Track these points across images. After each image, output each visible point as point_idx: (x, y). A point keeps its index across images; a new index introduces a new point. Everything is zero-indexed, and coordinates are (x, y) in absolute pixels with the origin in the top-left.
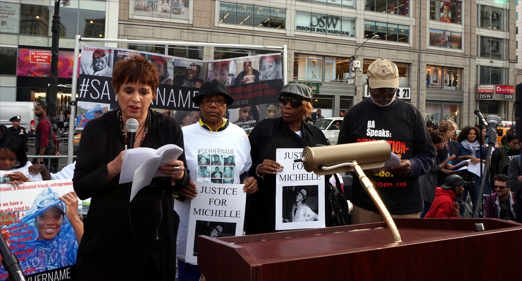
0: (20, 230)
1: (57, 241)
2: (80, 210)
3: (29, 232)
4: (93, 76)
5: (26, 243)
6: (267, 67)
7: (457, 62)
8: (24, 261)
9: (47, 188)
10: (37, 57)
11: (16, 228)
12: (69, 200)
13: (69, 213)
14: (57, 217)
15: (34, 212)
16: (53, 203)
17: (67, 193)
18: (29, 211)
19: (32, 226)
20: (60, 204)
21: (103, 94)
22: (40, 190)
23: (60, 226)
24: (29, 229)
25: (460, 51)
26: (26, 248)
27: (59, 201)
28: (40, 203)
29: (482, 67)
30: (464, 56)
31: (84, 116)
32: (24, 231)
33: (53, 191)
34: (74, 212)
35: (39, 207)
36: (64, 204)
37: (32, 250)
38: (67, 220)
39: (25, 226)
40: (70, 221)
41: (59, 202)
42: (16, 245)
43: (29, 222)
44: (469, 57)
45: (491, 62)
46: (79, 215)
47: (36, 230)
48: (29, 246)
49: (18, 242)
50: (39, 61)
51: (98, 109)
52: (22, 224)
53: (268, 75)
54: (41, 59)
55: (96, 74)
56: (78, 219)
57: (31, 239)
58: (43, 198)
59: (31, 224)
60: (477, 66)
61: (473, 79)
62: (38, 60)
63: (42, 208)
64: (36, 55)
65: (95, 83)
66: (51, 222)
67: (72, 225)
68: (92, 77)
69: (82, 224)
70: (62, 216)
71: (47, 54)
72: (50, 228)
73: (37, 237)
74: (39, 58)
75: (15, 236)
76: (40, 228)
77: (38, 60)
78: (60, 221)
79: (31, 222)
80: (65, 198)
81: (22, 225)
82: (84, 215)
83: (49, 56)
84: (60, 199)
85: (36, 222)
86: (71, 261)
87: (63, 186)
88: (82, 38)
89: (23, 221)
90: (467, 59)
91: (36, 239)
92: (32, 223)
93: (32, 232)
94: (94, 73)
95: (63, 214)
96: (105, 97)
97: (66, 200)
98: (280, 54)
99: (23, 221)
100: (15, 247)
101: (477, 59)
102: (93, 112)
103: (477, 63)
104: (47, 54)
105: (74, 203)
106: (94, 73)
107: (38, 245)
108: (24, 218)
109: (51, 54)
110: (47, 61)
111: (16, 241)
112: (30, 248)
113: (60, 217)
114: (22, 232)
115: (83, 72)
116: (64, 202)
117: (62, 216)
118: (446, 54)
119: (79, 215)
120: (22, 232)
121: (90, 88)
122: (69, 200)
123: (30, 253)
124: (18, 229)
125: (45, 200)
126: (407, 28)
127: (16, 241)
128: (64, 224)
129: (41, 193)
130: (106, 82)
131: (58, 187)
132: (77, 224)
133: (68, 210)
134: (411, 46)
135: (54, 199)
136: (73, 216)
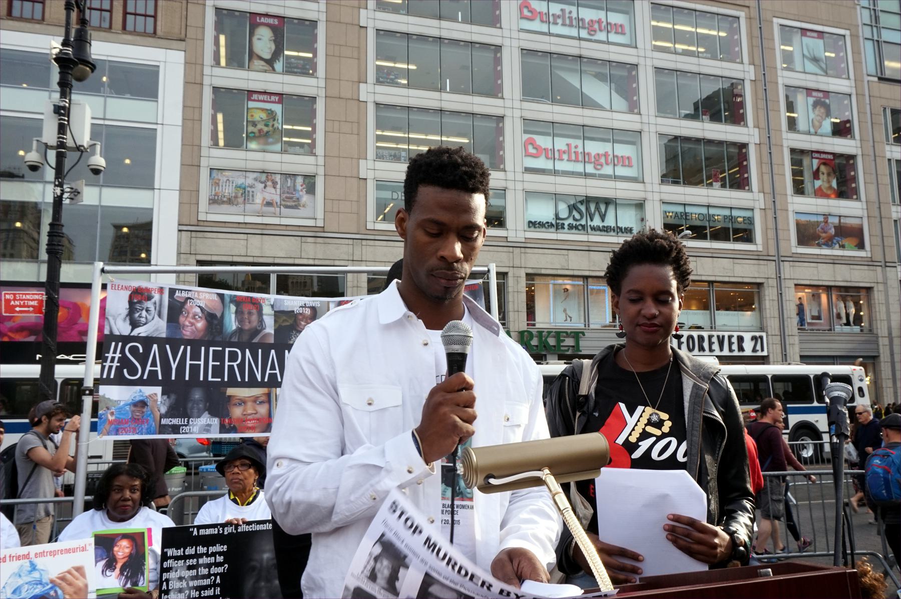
7: (858, 277)
9: (26, 560)
10: (17, 303)
12: (70, 584)
16: (38, 590)
17: (66, 570)
20: (52, 593)
25: (862, 254)
27: (50, 586)
28: (14, 592)
33: (39, 566)
36: (60, 592)
41: (51, 588)
44: (882, 264)
50: (21, 312)
54: (24, 306)
58: (20, 582)
62: (18, 309)
64: (15, 300)
74: (20, 306)
77: (18, 309)
80: (63, 579)
83: (42, 301)
84: (52, 581)
87: (59, 557)
90: (879, 269)
97: (64, 584)
98: (480, 281)
104: (36, 297)
105: (80, 589)
109: (44, 298)
110: (37, 310)
116: (61, 588)
118: (834, 261)
122: (70, 584)
125: (22, 585)
126: (748, 214)
129: (16, 571)
131: (49, 558)
134: (760, 248)
135: (40, 583)
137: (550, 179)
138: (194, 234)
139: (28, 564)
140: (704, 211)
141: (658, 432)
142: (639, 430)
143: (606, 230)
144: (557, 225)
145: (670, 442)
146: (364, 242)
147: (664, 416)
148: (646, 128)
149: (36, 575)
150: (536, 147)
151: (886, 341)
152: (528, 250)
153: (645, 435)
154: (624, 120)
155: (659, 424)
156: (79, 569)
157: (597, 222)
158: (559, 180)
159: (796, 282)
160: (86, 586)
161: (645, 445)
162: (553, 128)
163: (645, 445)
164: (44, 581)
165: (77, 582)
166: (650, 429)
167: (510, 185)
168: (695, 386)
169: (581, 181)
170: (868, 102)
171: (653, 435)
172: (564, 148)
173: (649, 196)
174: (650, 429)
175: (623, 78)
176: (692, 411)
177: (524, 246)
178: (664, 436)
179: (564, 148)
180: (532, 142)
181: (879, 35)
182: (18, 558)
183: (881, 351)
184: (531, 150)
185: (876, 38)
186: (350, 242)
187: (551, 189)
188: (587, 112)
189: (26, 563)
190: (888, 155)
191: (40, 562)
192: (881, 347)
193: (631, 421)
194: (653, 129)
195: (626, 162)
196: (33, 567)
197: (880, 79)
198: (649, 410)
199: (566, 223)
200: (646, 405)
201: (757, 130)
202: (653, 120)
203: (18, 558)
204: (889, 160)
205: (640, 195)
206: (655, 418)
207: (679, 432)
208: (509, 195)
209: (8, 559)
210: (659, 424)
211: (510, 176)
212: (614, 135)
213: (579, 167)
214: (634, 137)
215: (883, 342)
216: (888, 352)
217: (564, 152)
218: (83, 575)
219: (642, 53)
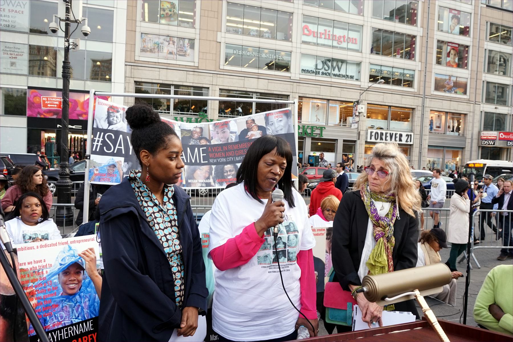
0: (45, 287)
3: (54, 288)
4: (107, 129)
5: (51, 299)
6: (275, 122)
7: (461, 108)
8: (51, 316)
9: (67, 245)
10: (49, 102)
11: (42, 285)
13: (88, 268)
14: (78, 273)
15: (56, 269)
16: (73, 260)
18: (52, 268)
19: (55, 282)
20: (80, 261)
21: (117, 147)
22: (62, 247)
23: (81, 281)
24: (53, 286)
25: (465, 97)
26: (52, 304)
27: (79, 257)
28: (62, 260)
29: (486, 113)
32: (49, 288)
34: (93, 268)
35: (61, 264)
36: (83, 260)
37: (57, 306)
38: (87, 275)
39: (49, 283)
42: (43, 301)
43: (53, 278)
45: (496, 108)
46: (98, 270)
47: (60, 286)
48: (55, 301)
49: (44, 298)
52: (46, 282)
53: (278, 129)
55: (111, 128)
57: (56, 295)
58: (65, 255)
59: (54, 281)
60: (481, 112)
62: (49, 105)
63: (64, 265)
64: (47, 100)
65: (109, 137)
66: (72, 278)
68: (105, 131)
69: (101, 278)
70: (82, 272)
71: (58, 100)
72: (72, 284)
73: (61, 293)
74: (50, 104)
75: (41, 292)
76: (64, 284)
77: (49, 105)
78: (81, 277)
79: (55, 279)
80: (84, 254)
81: (47, 282)
82: (102, 270)
84: (79, 255)
85: (59, 278)
87: (82, 243)
89: (47, 278)
90: (472, 105)
91: (60, 295)
92: (55, 280)
93: (56, 288)
94: (109, 126)
95: (84, 270)
97: (85, 256)
99: (47, 278)
100: (42, 303)
101: (482, 105)
103: (482, 109)
104: (58, 100)
105: (93, 259)
106: (109, 126)
107: (62, 300)
108: (48, 275)
109: (62, 100)
111: (42, 297)
112: (55, 303)
113: (80, 273)
114: (47, 288)
117: (82, 272)
118: (451, 100)
119: (98, 270)
120: (47, 288)
121: (104, 142)
122: (88, 257)
123: (55, 308)
124: (43, 285)
126: (412, 73)
127: (42, 297)
128: (84, 279)
129: (62, 250)
130: (121, 136)
131: (77, 244)
133: (88, 266)
134: (416, 91)
136: (92, 271)
137: (315, 48)
139: (68, 247)
140: (390, 69)
143: (339, 76)
148: (366, 24)
149: (72, 252)
150: (309, 31)
151: (470, 141)
156: (91, 249)
157: (336, 72)
158: (319, 48)
159: (431, 109)
160: (95, 257)
162: (318, 20)
164: (76, 255)
165: (91, 255)
167: (294, 50)
170: (479, 18)
172: (323, 32)
173: (364, 60)
177: (298, 82)
179: (323, 32)
180: (306, 27)
182: (63, 244)
183: (467, 145)
184: (306, 32)
187: (314, 53)
188: (336, 13)
189: (66, 246)
190: (485, 47)
191: (73, 246)
192: (467, 143)
194: (369, 24)
195: (354, 41)
196: (70, 248)
197: (487, 6)
199: (321, 71)
201: (422, 29)
202: (370, 19)
203: (63, 244)
204: (486, 49)
205: (358, 60)
208: (293, 55)
209: (58, 244)
211: (294, 45)
213: (329, 43)
215: (468, 141)
218: (94, 252)
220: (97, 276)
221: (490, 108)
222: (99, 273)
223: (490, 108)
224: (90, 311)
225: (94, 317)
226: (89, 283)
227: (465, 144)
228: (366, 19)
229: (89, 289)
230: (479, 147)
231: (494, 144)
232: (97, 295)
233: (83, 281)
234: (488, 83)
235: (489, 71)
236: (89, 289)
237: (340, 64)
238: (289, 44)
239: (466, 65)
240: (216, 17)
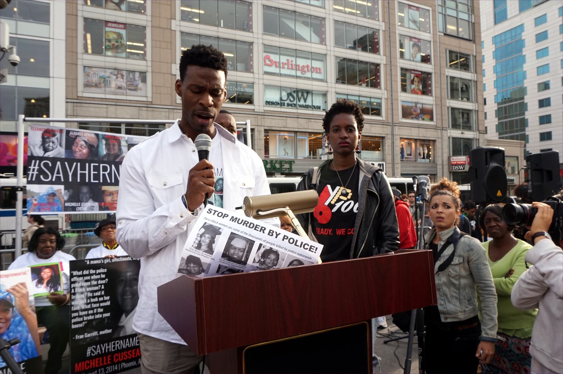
1: (7, 335)
2: (31, 302)
7: (429, 135)
12: (18, 292)
14: (6, 311)
20: (8, 297)
25: (432, 123)
29: (453, 138)
30: (436, 128)
31: (35, 200)
36: (12, 296)
40: (21, 314)
41: (7, 294)
45: (462, 133)
46: (31, 307)
51: (50, 192)
56: (29, 310)
60: (449, 137)
61: (446, 150)
67: (24, 317)
78: (10, 315)
80: (14, 289)
84: (7, 291)
86: (25, 355)
87: (10, 278)
88: (27, 118)
90: (439, 131)
95: (13, 307)
96: (58, 178)
97: (14, 292)
101: (449, 131)
102: (46, 195)
103: (449, 134)
113: (9, 310)
115: (32, 154)
116: (13, 294)
117: (11, 309)
118: (419, 127)
126: (379, 101)
128: (14, 317)
132: (29, 316)
134: (384, 119)
137: (278, 78)
138: (75, 104)
140: (357, 98)
141: (345, 199)
142: (336, 198)
143: (307, 107)
144: (281, 104)
145: (350, 203)
146: (175, 111)
147: (349, 191)
148: (329, 53)
150: (270, 61)
152: (265, 117)
153: (339, 200)
154: (317, 48)
155: (346, 195)
156: (23, 284)
157: (302, 102)
158: (283, 79)
160: (28, 293)
161: (338, 205)
162: (280, 50)
163: (338, 205)
166: (342, 197)
167: (256, 81)
168: (365, 176)
169: (294, 80)
171: (342, 200)
172: (286, 62)
173: (330, 90)
174: (342, 197)
175: (317, 25)
176: (362, 188)
177: (264, 114)
178: (348, 200)
179: (286, 62)
181: (445, 11)
184: (268, 62)
185: (444, 13)
186: (167, 110)
187: (278, 84)
188: (298, 42)
190: (447, 74)
193: (332, 194)
194: (332, 53)
195: (318, 70)
197: (445, 34)
198: (342, 188)
199: (286, 102)
200: (341, 186)
201: (385, 57)
202: (332, 49)
204: (447, 76)
205: (325, 89)
206: (344, 192)
207: (355, 198)
208: (256, 86)
210: (346, 195)
211: (256, 76)
212: (312, 56)
213: (293, 73)
214: (322, 57)
215: (439, 167)
216: (441, 172)
217: (285, 64)
219: (327, 12)
220: (29, 313)
221: (457, 133)
222: (32, 310)
223: (457, 133)
224: (22, 353)
225: (26, 359)
226: (20, 321)
227: (437, 171)
228: (328, 48)
229: (20, 329)
230: (450, 172)
231: (464, 169)
232: (30, 335)
233: (12, 320)
234: (453, 109)
235: (453, 96)
236: (20, 329)
237: (305, 95)
238: (250, 75)
239: (430, 92)
240: (169, 47)
